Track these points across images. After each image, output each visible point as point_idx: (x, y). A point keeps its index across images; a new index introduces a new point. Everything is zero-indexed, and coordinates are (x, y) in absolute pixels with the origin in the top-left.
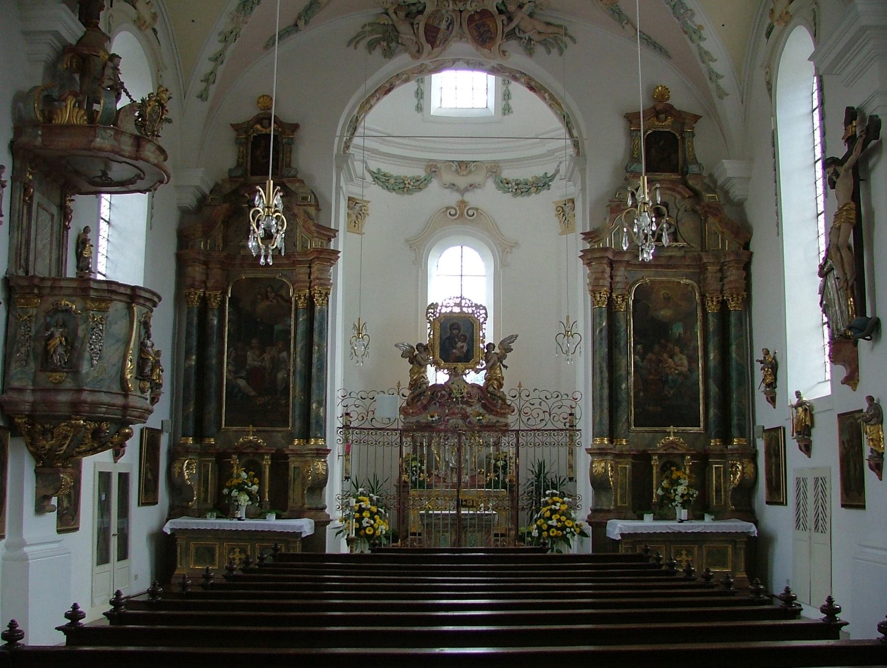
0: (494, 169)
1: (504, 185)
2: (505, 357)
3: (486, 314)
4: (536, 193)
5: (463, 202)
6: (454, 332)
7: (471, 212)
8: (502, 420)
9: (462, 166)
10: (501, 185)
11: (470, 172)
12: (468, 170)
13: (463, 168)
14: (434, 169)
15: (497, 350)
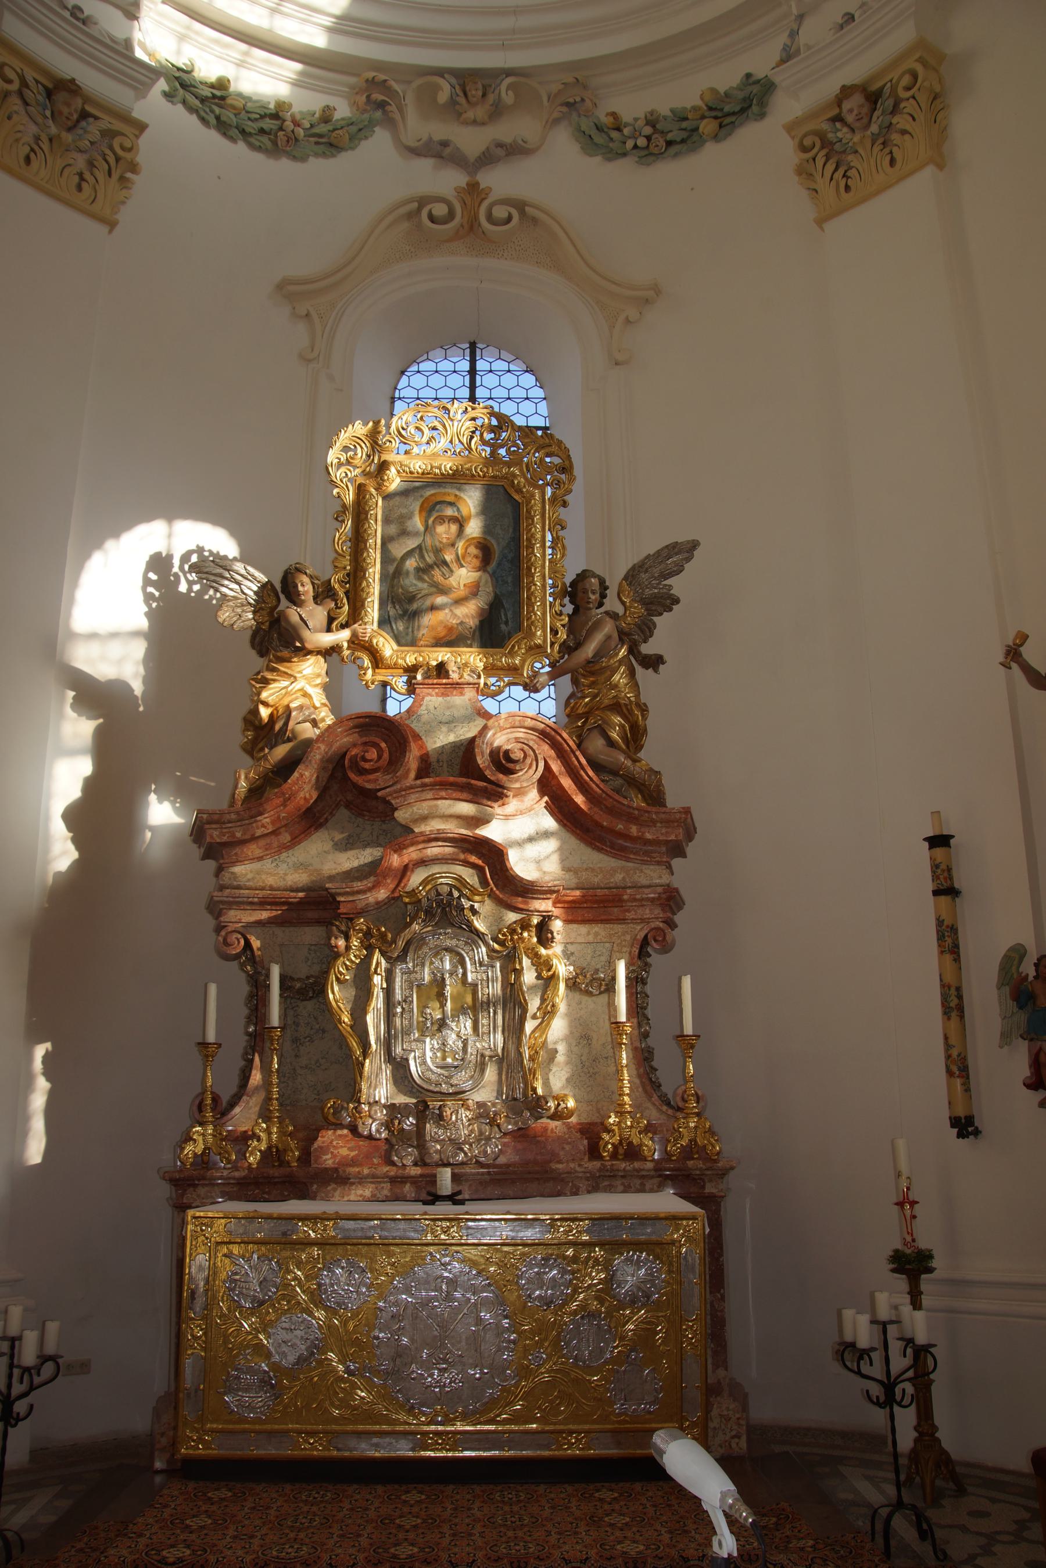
0: (571, 99)
1: (607, 139)
2: (647, 630)
3: (566, 468)
4: (716, 138)
5: (473, 188)
6: (440, 529)
7: (500, 212)
8: (652, 875)
9: (473, 90)
10: (599, 139)
11: (497, 112)
12: (491, 98)
13: (476, 93)
14: (378, 97)
15: (612, 603)
